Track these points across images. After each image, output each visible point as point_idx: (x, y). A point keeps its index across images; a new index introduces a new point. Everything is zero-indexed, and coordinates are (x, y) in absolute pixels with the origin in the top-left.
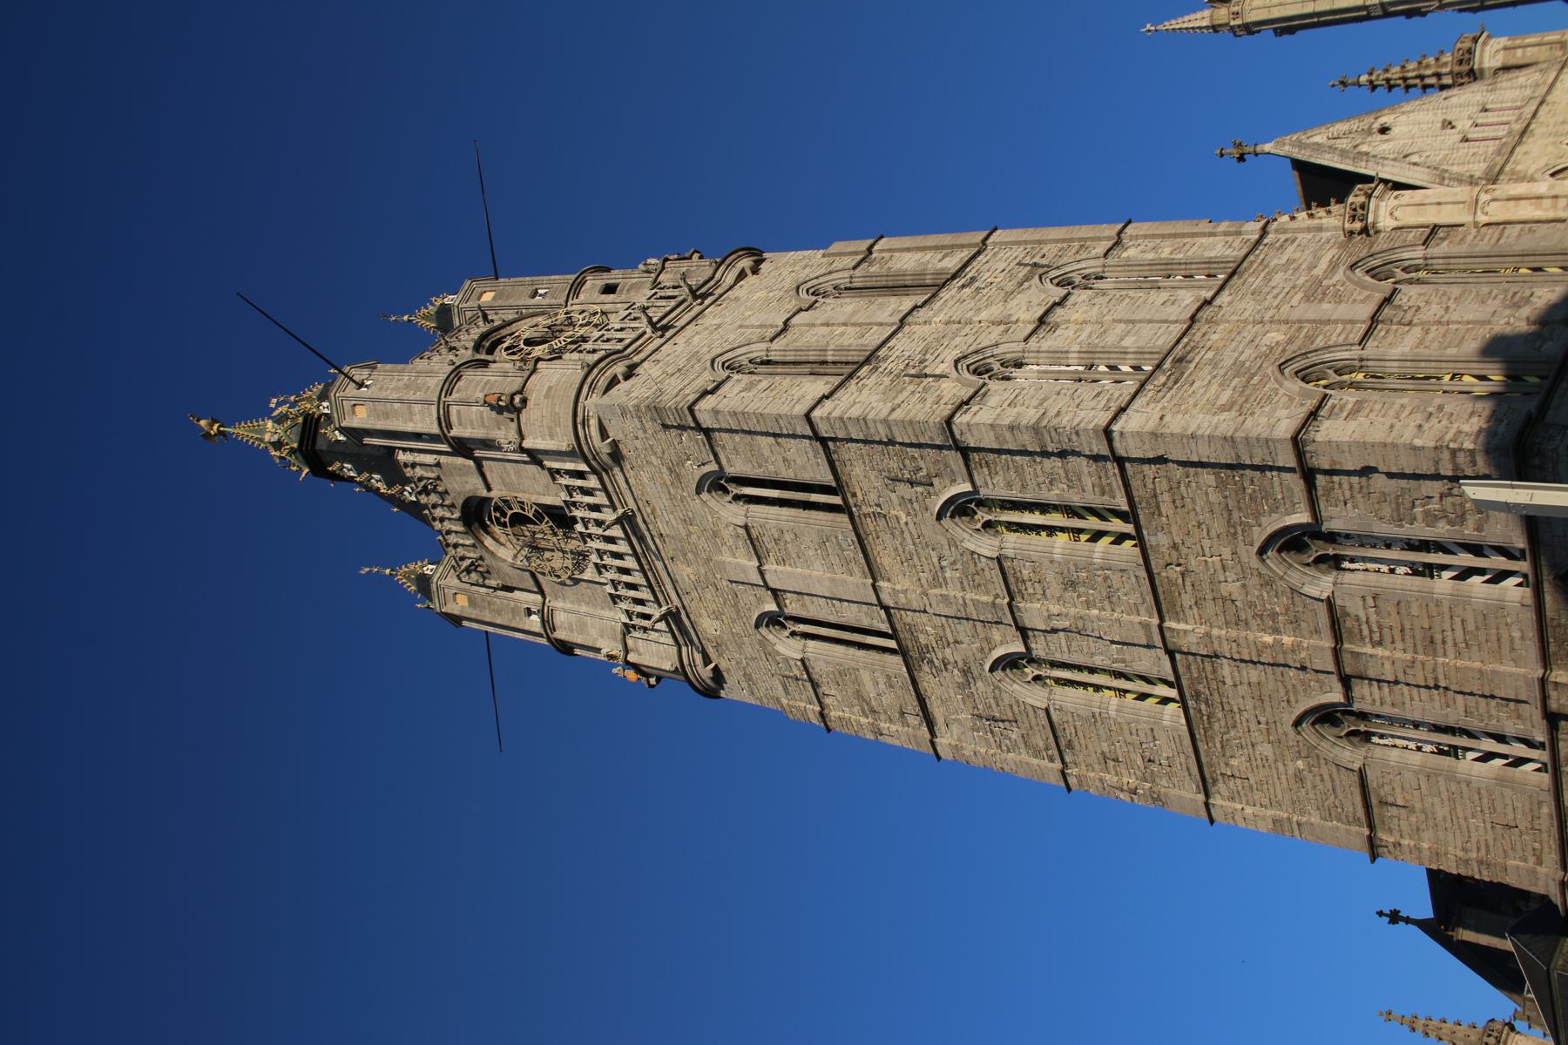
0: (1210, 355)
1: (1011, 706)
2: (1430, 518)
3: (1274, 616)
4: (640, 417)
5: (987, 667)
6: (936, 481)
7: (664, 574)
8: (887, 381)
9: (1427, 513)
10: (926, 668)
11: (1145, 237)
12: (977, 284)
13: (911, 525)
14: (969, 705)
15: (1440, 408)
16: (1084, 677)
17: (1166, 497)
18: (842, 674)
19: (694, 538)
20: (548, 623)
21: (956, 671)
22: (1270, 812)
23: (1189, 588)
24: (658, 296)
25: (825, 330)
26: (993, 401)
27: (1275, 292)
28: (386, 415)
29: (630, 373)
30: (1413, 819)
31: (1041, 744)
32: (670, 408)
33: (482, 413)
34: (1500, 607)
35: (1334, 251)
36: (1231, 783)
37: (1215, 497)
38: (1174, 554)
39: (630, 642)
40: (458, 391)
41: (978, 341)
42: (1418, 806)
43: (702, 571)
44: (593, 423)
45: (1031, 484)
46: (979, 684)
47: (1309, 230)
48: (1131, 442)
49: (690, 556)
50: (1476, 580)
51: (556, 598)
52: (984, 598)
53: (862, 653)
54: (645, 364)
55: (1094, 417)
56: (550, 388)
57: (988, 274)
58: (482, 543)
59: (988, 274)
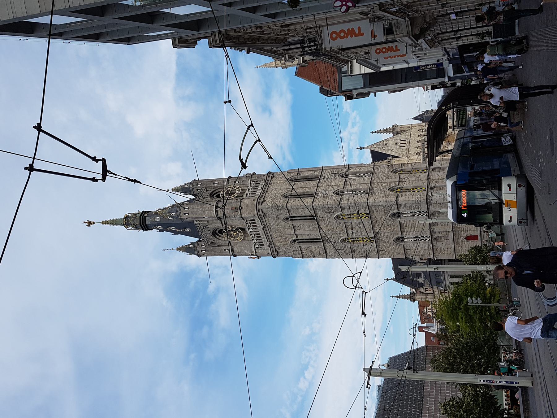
0: (376, 189)
1: (343, 247)
4: (272, 209)
5: (339, 241)
6: (334, 212)
8: (322, 197)
10: (327, 243)
11: (353, 167)
12: (326, 178)
15: (414, 194)
17: (375, 210)
19: (279, 228)
23: (377, 222)
24: (255, 183)
25: (301, 189)
26: (344, 199)
27: (381, 177)
28: (196, 214)
30: (411, 251)
31: (348, 252)
32: (281, 206)
33: (228, 211)
35: (387, 169)
36: (382, 252)
37: (382, 210)
38: (375, 218)
39: (257, 251)
41: (334, 189)
42: (412, 249)
44: (260, 210)
45: (352, 211)
46: (337, 244)
47: (381, 165)
48: (371, 203)
50: (420, 216)
54: (265, 198)
55: (364, 200)
56: (247, 205)
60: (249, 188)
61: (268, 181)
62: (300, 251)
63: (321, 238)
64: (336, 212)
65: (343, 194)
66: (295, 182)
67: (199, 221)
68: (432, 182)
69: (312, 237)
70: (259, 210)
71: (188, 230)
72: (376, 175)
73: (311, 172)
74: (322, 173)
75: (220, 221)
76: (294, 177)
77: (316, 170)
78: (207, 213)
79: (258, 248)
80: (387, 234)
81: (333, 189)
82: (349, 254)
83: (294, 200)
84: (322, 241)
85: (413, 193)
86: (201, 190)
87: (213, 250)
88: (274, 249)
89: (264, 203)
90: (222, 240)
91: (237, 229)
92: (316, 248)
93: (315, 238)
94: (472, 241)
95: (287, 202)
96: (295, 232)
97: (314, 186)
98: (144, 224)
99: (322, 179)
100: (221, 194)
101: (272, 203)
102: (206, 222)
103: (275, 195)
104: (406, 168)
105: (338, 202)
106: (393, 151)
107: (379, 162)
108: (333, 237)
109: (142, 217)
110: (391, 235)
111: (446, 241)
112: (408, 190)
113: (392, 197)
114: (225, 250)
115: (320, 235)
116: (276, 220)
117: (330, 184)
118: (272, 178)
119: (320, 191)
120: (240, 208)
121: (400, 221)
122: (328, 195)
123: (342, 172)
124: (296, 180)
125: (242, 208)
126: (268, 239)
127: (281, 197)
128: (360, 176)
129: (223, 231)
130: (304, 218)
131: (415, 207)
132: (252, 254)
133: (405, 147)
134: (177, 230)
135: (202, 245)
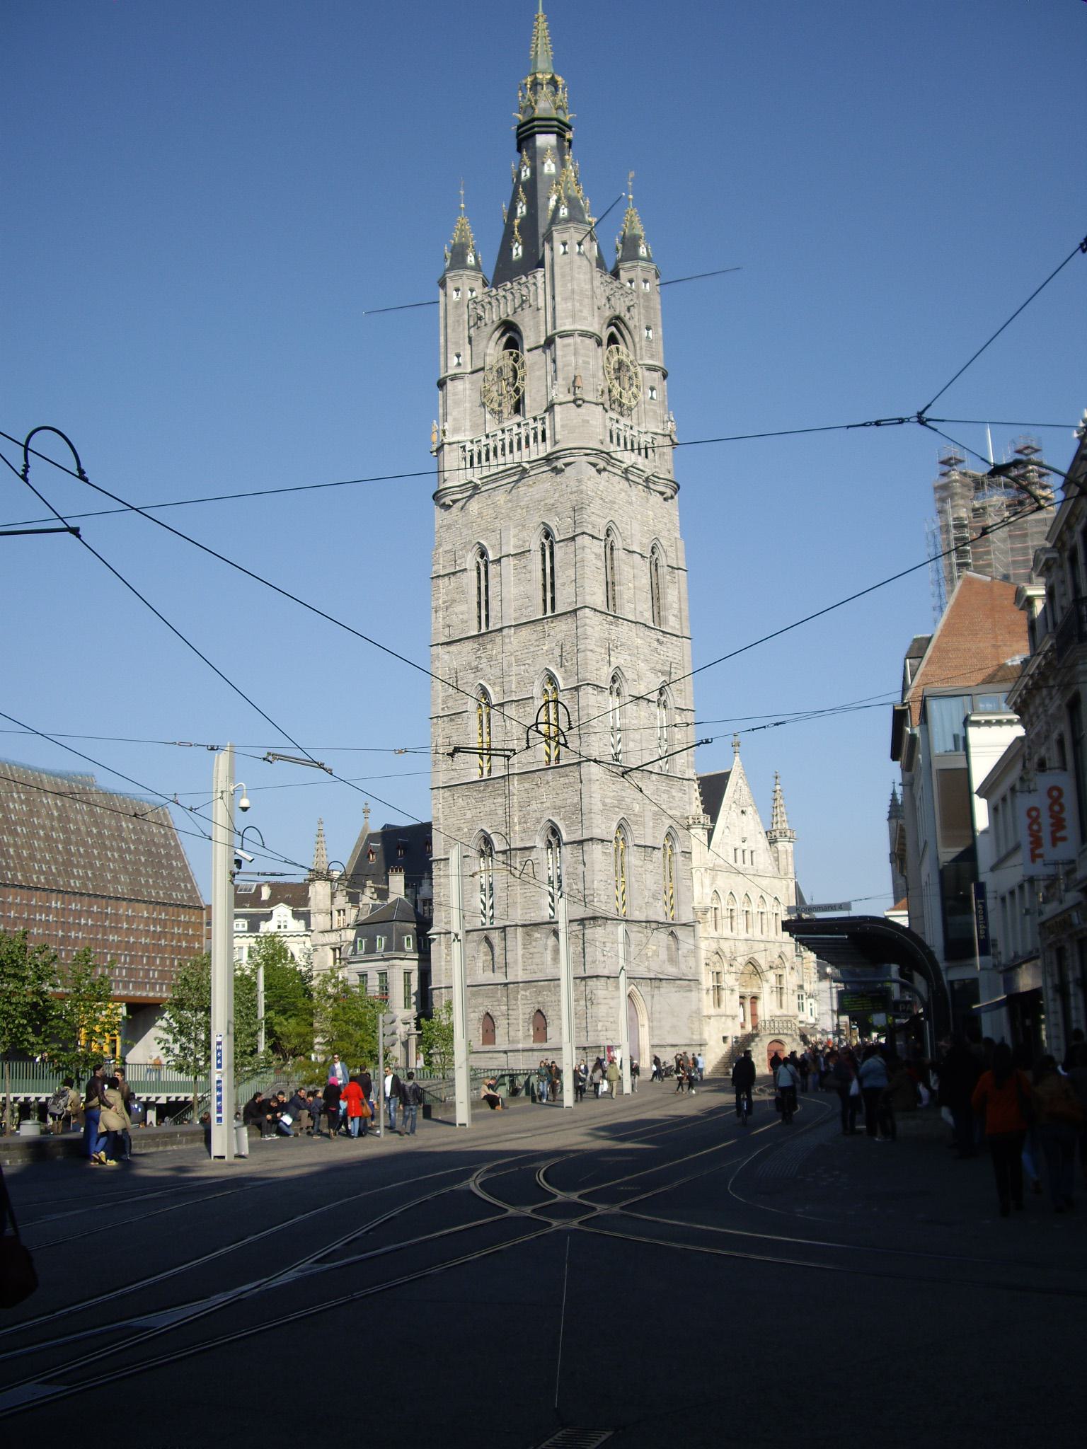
2: (569, 885)
3: (526, 822)
5: (482, 682)
6: (563, 669)
7: (498, 484)
8: (606, 635)
9: (571, 884)
10: (476, 646)
13: (541, 652)
14: (462, 668)
15: (610, 884)
16: (485, 730)
17: (567, 781)
18: (461, 590)
19: (519, 511)
20: (454, 378)
21: (476, 663)
22: (441, 815)
26: (600, 698)
28: (563, 276)
29: (599, 471)
31: (449, 705)
34: (540, 909)
35: (678, 814)
37: (569, 801)
39: (455, 445)
40: (582, 341)
41: (629, 670)
43: (503, 511)
46: (473, 675)
49: (510, 505)
50: (550, 899)
51: (472, 383)
52: (513, 686)
53: (475, 605)
56: (588, 422)
57: (665, 649)
58: (496, 330)
59: (665, 649)
60: (636, 428)
61: (654, 483)
62: (453, 571)
63: (490, 629)
64: (564, 675)
65: (615, 694)
66: (648, 560)
67: (545, 282)
68: (640, 932)
69: (494, 604)
70: (572, 455)
71: (517, 251)
72: (664, 784)
73: (676, 606)
74: (672, 637)
75: (542, 343)
76: (664, 558)
77: (681, 618)
78: (564, 306)
79: (464, 451)
80: (500, 812)
81: (629, 665)
82: (443, 709)
83: (600, 555)
84: (482, 631)
85: (613, 883)
86: (629, 292)
87: (458, 321)
88: (459, 496)
89: (594, 470)
90: (487, 347)
91: (517, 391)
92: (461, 617)
93: (491, 614)
94: (481, 1031)
95: (593, 537)
96: (508, 556)
97: (638, 612)
98: (536, 129)
99: (655, 637)
100: (618, 349)
101: (593, 494)
102: (541, 304)
103: (615, 503)
104: (680, 863)
105: (592, 678)
106: (727, 830)
107: (697, 794)
108: (492, 663)
109: (555, 123)
110: (495, 824)
111: (481, 965)
112: (621, 870)
113: (603, 826)
114: (458, 356)
115: (499, 626)
116: (542, 503)
117: (642, 657)
118: (662, 493)
119: (624, 630)
120: (580, 402)
121: (535, 847)
122: (612, 653)
123: (674, 693)
124: (653, 562)
125: (579, 406)
126: (489, 479)
127: (608, 519)
128: (663, 741)
129: (515, 351)
130: (549, 584)
131: (575, 887)
132: (447, 433)
133: (736, 862)
134: (517, 222)
135: (472, 290)
